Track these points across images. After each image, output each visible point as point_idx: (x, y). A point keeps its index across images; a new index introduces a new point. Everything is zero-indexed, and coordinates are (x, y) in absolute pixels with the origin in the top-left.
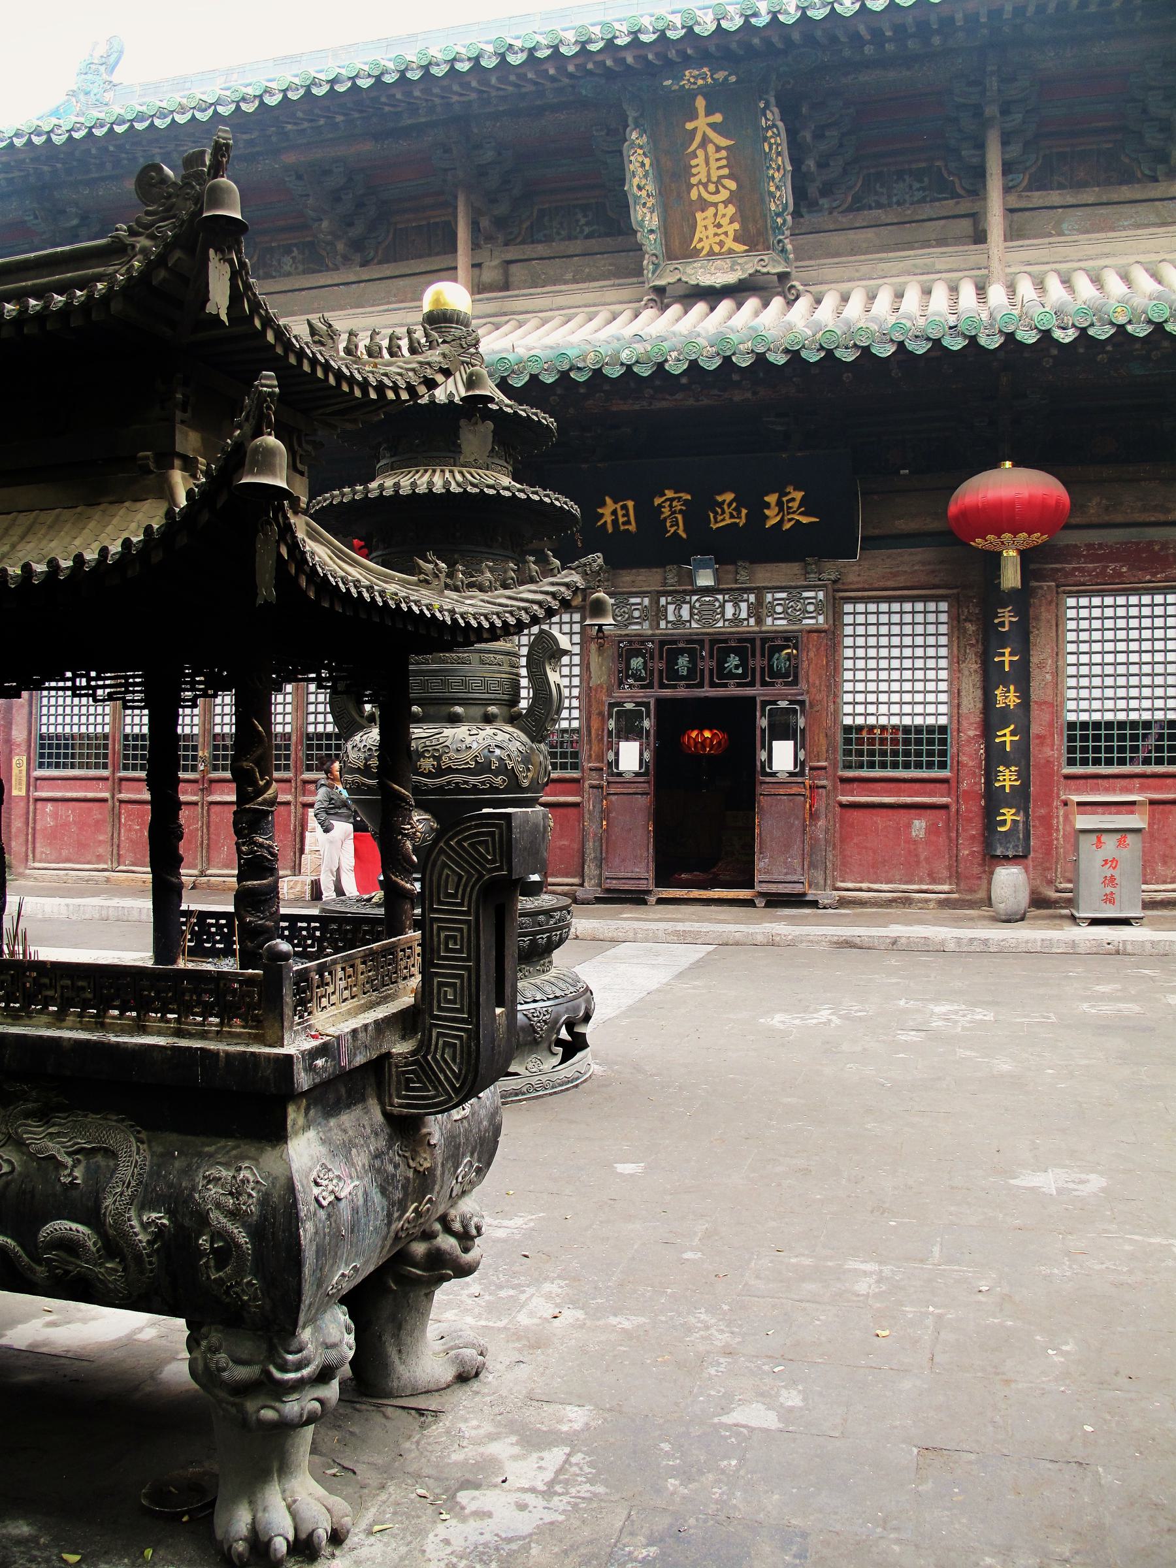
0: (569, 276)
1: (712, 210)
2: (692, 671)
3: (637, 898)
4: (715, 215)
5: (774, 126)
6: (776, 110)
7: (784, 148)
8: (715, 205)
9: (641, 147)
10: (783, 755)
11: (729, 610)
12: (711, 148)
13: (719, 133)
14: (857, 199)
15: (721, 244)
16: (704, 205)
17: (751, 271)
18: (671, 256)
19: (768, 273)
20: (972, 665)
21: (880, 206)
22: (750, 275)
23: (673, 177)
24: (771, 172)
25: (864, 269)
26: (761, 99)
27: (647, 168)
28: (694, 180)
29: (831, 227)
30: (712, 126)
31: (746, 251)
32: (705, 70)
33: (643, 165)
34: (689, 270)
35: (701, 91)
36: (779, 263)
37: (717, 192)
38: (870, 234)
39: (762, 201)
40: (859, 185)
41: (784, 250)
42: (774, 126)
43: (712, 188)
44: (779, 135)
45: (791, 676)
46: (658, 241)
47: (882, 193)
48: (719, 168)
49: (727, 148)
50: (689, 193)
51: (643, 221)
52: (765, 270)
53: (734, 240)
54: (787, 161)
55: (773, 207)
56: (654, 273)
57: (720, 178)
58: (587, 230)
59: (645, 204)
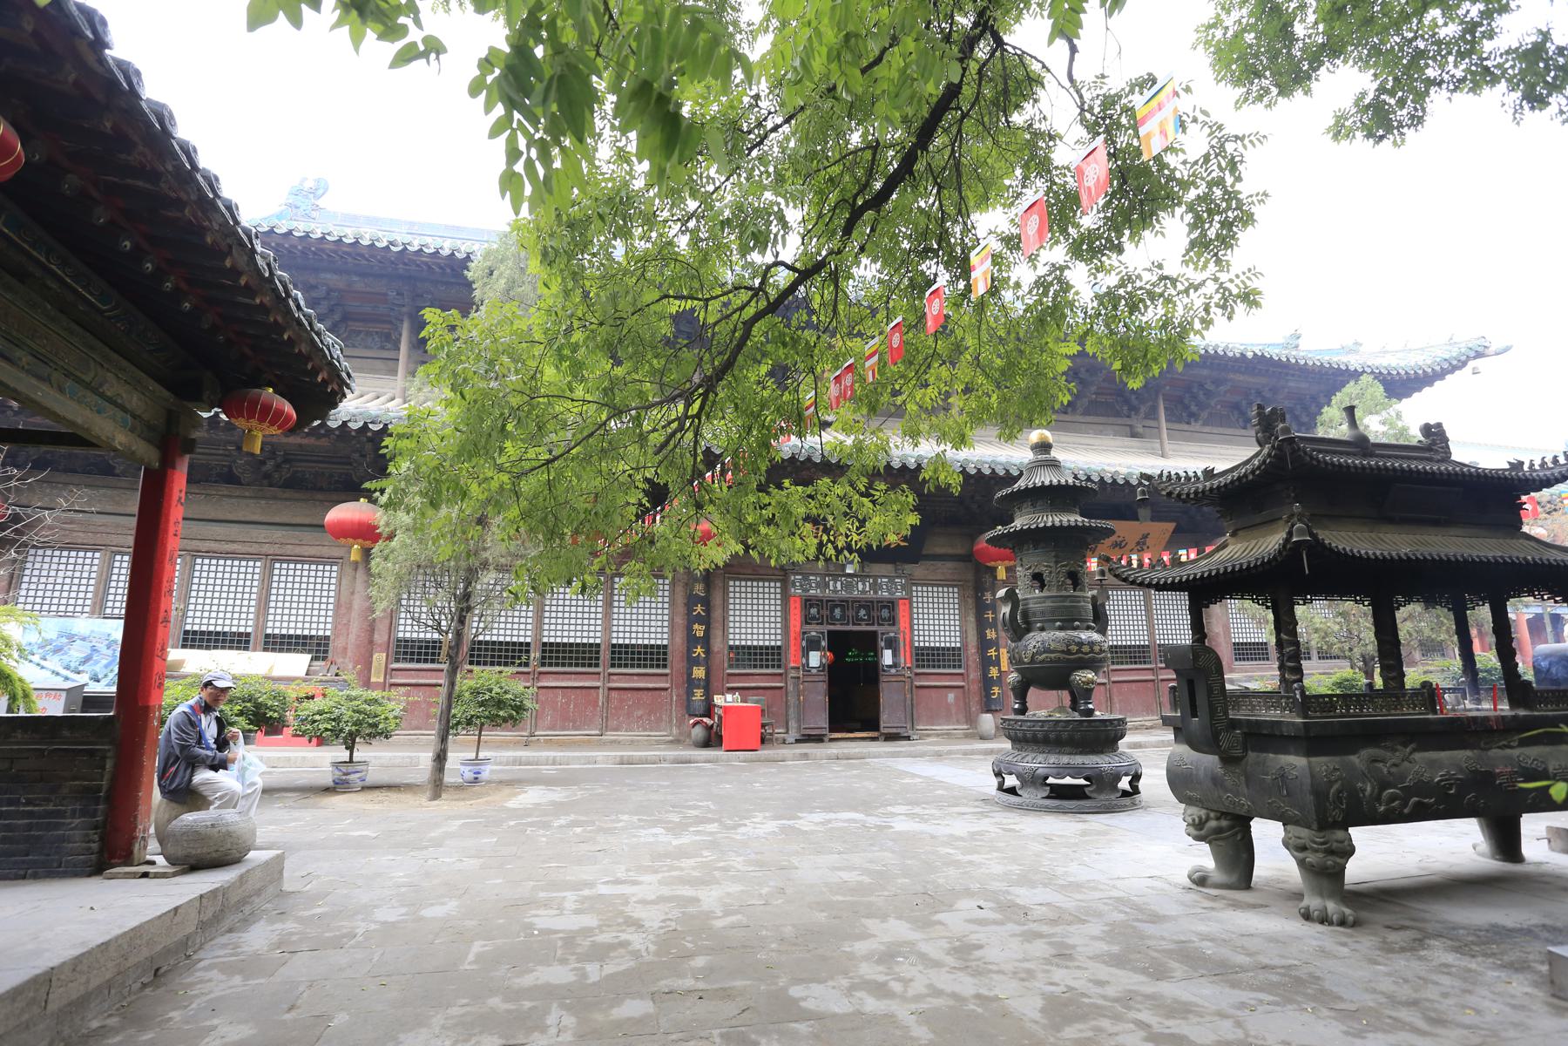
2: (843, 617)
3: (819, 739)
10: (887, 658)
11: (860, 586)
20: (972, 618)
45: (892, 621)
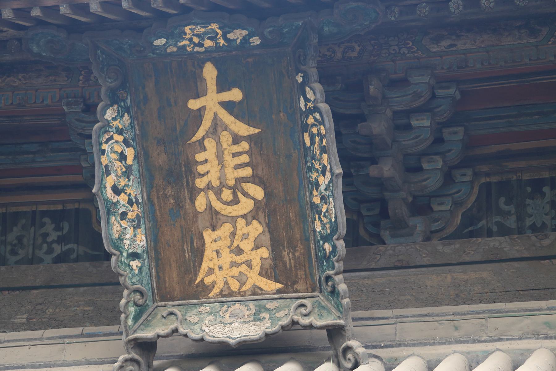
0: (21, 319)
1: (227, 228)
5: (316, 109)
6: (318, 86)
7: (330, 141)
8: (233, 220)
9: (120, 132)
12: (226, 138)
13: (237, 117)
14: (470, 219)
15: (242, 279)
16: (214, 219)
17: (285, 322)
18: (164, 295)
19: (310, 327)
21: (504, 231)
22: (283, 327)
23: (169, 175)
24: (314, 175)
25: (468, 326)
26: (298, 71)
27: (130, 161)
28: (200, 183)
29: (426, 261)
30: (228, 106)
31: (279, 291)
32: (214, 26)
33: (122, 157)
34: (192, 317)
35: (210, 56)
36: (328, 311)
37: (236, 201)
38: (487, 273)
39: (303, 217)
40: (473, 198)
41: (334, 292)
42: (316, 109)
43: (227, 195)
44: (322, 123)
46: (145, 270)
47: (509, 213)
48: (238, 167)
49: (250, 138)
51: (121, 239)
52: (305, 321)
53: (260, 274)
54: (336, 159)
56: (136, 318)
57: (240, 180)
58: (58, 249)
59: (124, 216)
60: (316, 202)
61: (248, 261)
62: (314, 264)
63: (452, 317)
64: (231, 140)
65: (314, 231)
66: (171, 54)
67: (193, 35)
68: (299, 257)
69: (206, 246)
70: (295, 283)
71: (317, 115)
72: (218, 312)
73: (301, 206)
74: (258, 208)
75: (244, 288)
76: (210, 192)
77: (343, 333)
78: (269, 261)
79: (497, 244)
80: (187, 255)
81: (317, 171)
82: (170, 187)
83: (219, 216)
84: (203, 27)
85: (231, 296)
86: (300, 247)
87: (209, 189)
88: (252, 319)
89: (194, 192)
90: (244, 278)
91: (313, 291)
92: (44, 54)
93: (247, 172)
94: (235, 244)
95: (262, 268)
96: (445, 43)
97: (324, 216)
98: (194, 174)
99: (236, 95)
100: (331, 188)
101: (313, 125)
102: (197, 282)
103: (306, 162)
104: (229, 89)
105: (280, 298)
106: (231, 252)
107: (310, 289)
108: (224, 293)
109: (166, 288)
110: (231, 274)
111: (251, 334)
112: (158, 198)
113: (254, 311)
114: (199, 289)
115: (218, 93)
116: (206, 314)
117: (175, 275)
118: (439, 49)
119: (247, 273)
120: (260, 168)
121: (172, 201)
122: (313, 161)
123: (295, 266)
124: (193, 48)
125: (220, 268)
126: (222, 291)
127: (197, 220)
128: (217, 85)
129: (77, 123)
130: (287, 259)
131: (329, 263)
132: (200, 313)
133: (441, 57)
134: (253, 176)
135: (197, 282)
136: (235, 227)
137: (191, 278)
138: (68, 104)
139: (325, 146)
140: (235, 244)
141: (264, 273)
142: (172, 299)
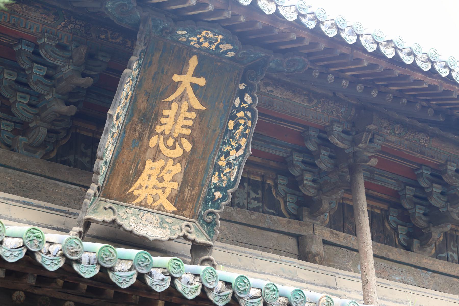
4: (163, 168)
13: (196, 96)
16: (157, 154)
23: (145, 119)
24: (227, 148)
25: (246, 260)
28: (159, 129)
30: (195, 87)
31: (174, 212)
37: (173, 148)
39: (206, 170)
43: (170, 142)
50: (149, 138)
53: (168, 198)
55: (215, 180)
57: (182, 136)
60: (220, 165)
61: (164, 187)
62: (201, 201)
63: (237, 253)
64: (187, 108)
65: (210, 181)
66: (179, 42)
67: (204, 37)
68: (193, 195)
69: (145, 170)
70: (184, 210)
71: (249, 114)
72: (138, 215)
73: (208, 164)
74: (184, 156)
75: (155, 204)
76: (162, 137)
77: (208, 250)
78: (176, 192)
79: (230, 211)
80: (131, 172)
81: (232, 146)
82: (140, 125)
83: (161, 154)
84: (214, 35)
85: (146, 207)
86: (197, 189)
87: (162, 134)
88: (158, 226)
89: (152, 133)
90: (157, 198)
91: (192, 218)
92: (110, 10)
93: (188, 132)
94: (161, 175)
95: (170, 195)
96: (269, 88)
97: (225, 175)
98: (158, 122)
99: (201, 82)
100: (240, 160)
101: (241, 118)
102: (129, 191)
103: (224, 138)
104: (199, 77)
105: (174, 217)
106: (158, 178)
107: (191, 216)
108: (142, 204)
109: (109, 189)
110: (151, 193)
111: (159, 236)
112: (130, 129)
113: (159, 221)
114: (129, 196)
115: (192, 76)
116: (130, 215)
117: (118, 183)
118: (264, 90)
119: (161, 195)
120: (196, 132)
121: (137, 134)
122: (231, 140)
123: (189, 200)
124: (195, 44)
125: (147, 187)
126: (141, 202)
127: (146, 151)
128: (194, 71)
129: (52, 53)
130: (186, 194)
131: (214, 205)
132: (127, 213)
133: (261, 95)
134: (190, 135)
135: (129, 191)
136: (166, 164)
137: (127, 188)
138: (49, 38)
139: (247, 134)
140: (161, 175)
141: (170, 198)
142: (109, 198)
